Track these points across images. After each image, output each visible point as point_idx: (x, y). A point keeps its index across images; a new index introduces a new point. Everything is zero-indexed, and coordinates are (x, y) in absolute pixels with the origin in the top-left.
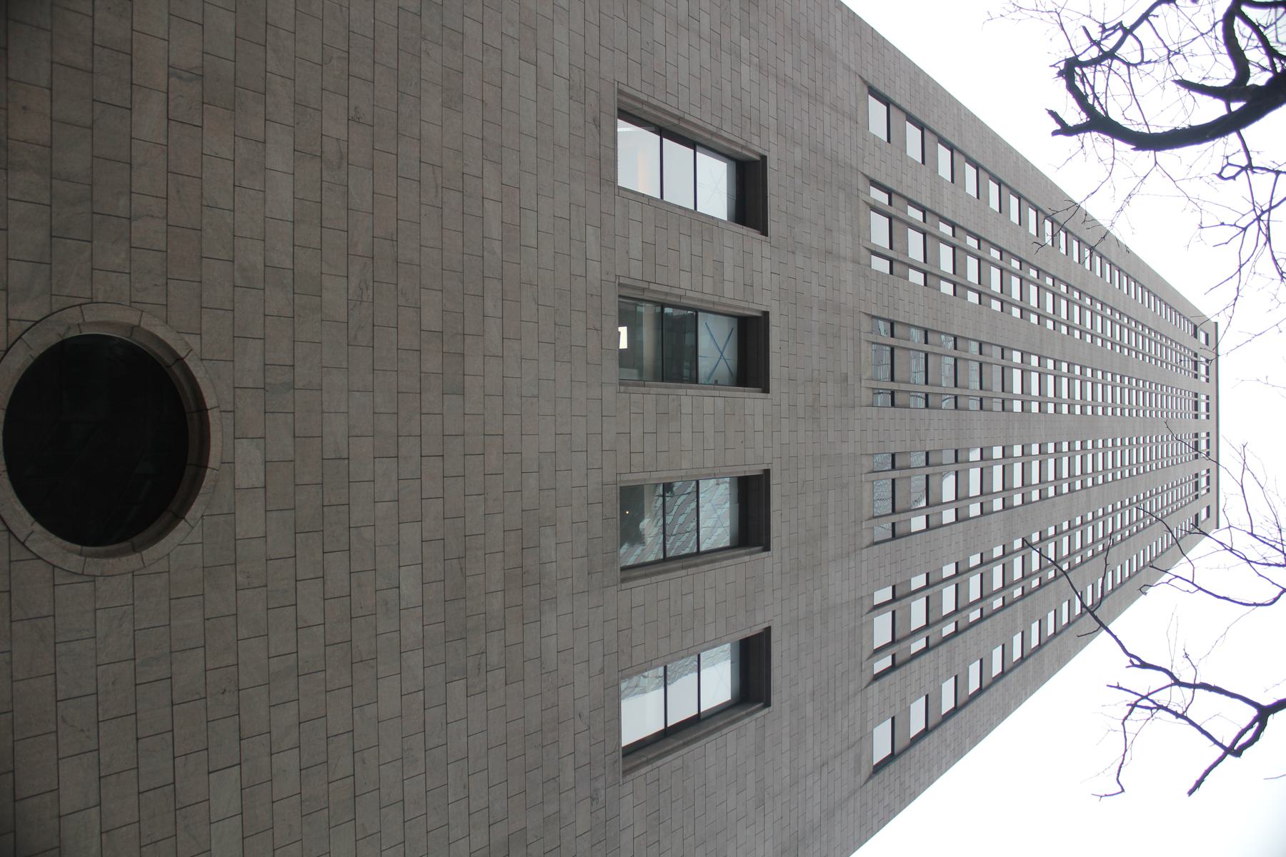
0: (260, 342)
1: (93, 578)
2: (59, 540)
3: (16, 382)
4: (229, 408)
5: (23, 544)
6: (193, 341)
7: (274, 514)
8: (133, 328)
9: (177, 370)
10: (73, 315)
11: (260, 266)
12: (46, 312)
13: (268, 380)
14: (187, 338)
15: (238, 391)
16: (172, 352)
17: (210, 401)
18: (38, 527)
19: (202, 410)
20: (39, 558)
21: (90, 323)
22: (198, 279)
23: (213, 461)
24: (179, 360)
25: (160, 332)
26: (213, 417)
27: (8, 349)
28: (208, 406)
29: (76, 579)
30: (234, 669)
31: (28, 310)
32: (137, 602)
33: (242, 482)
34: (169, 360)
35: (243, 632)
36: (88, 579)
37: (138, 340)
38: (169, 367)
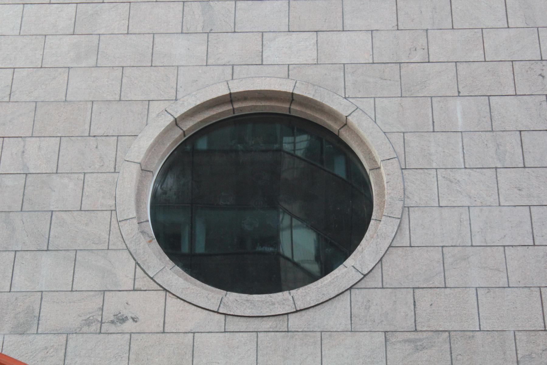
0: (158, 39)
1: (406, 208)
2: (363, 242)
3: (198, 282)
4: (229, 70)
5: (365, 276)
6: (156, 108)
7: (347, 22)
8: (144, 171)
9: (188, 125)
10: (130, 229)
11: (75, 39)
12: (126, 254)
13: (199, 29)
14: (152, 115)
15: (210, 62)
16: (167, 130)
17: (222, 91)
18: (349, 262)
19: (231, 98)
20: (381, 260)
21: (138, 211)
22: (90, 105)
23: (286, 87)
24: (176, 123)
25: (146, 141)
26: (237, 87)
27: (165, 290)
28: (227, 92)
29: (405, 226)
30: (517, 65)
31: (124, 272)
32: (434, 165)
33: (310, 56)
34: (177, 134)
35: (477, 55)
36: (406, 216)
37: (157, 166)
38: (184, 133)
